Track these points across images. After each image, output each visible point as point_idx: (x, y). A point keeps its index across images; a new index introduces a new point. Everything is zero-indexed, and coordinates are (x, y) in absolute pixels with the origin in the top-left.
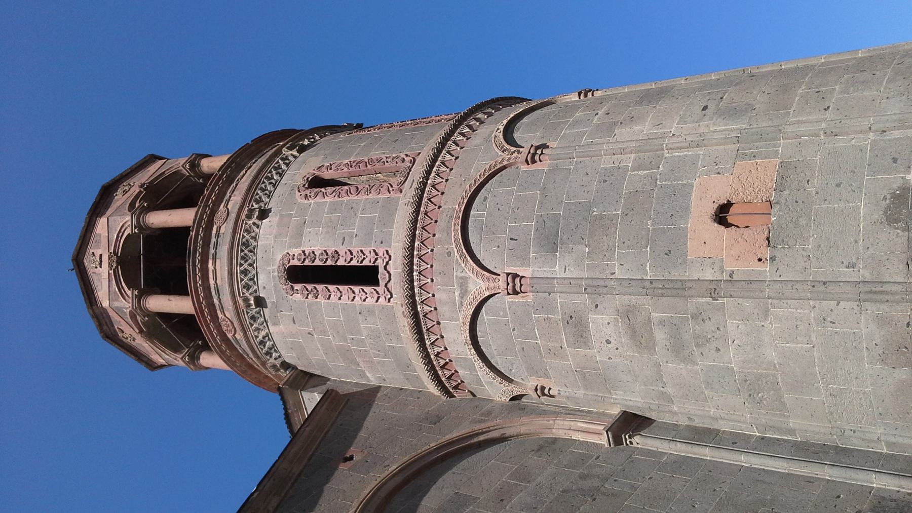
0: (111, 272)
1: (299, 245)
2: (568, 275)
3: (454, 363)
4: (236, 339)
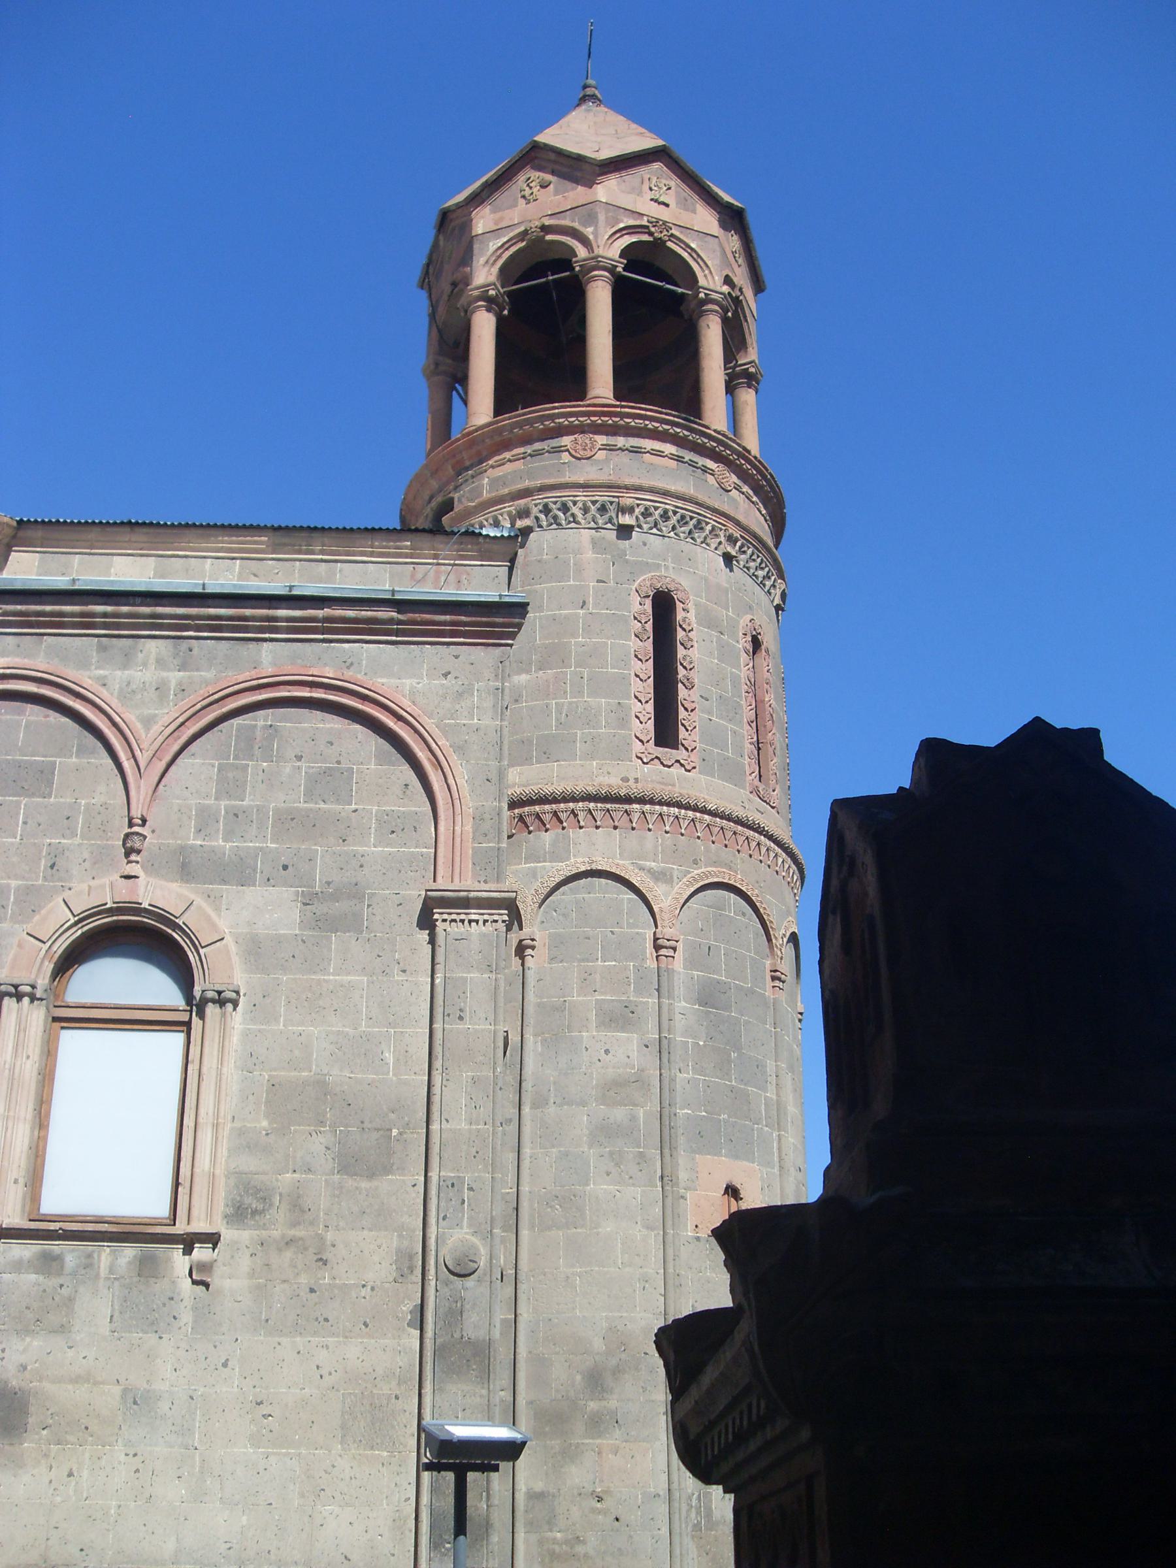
0: (644, 222)
2: (678, 1017)
3: (560, 831)
4: (562, 451)
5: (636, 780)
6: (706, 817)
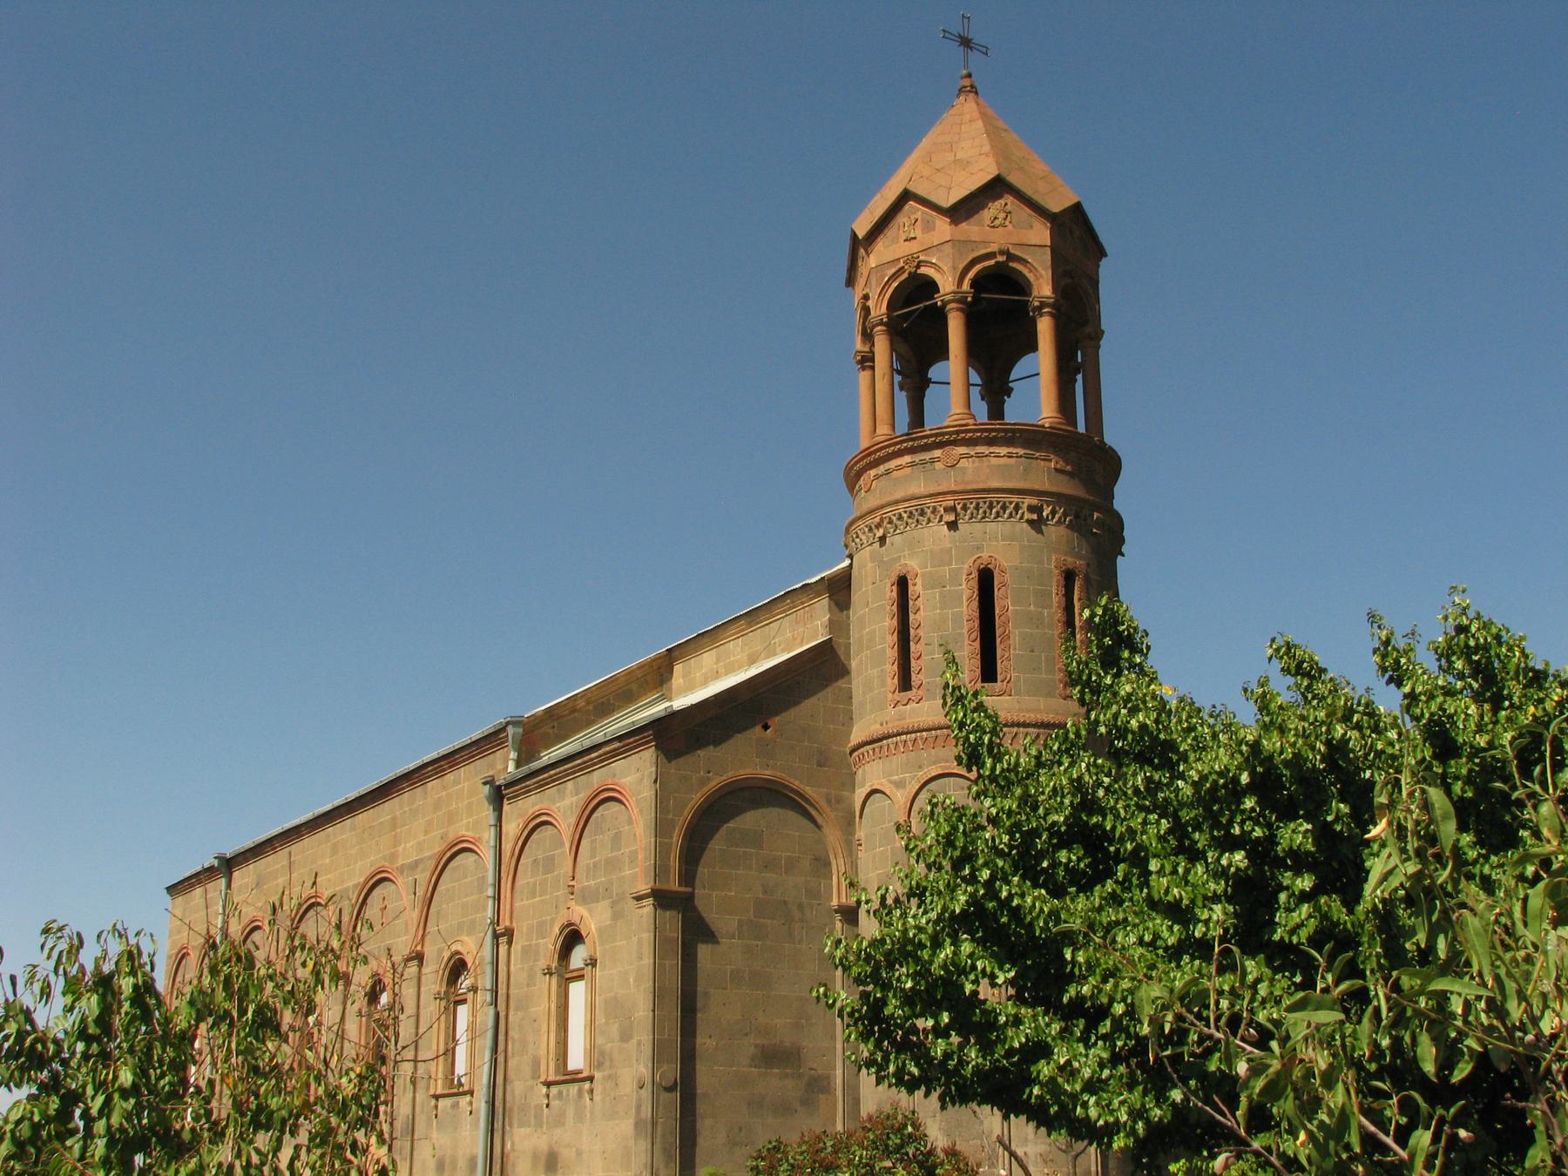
0: (902, 264)
1: (925, 588)
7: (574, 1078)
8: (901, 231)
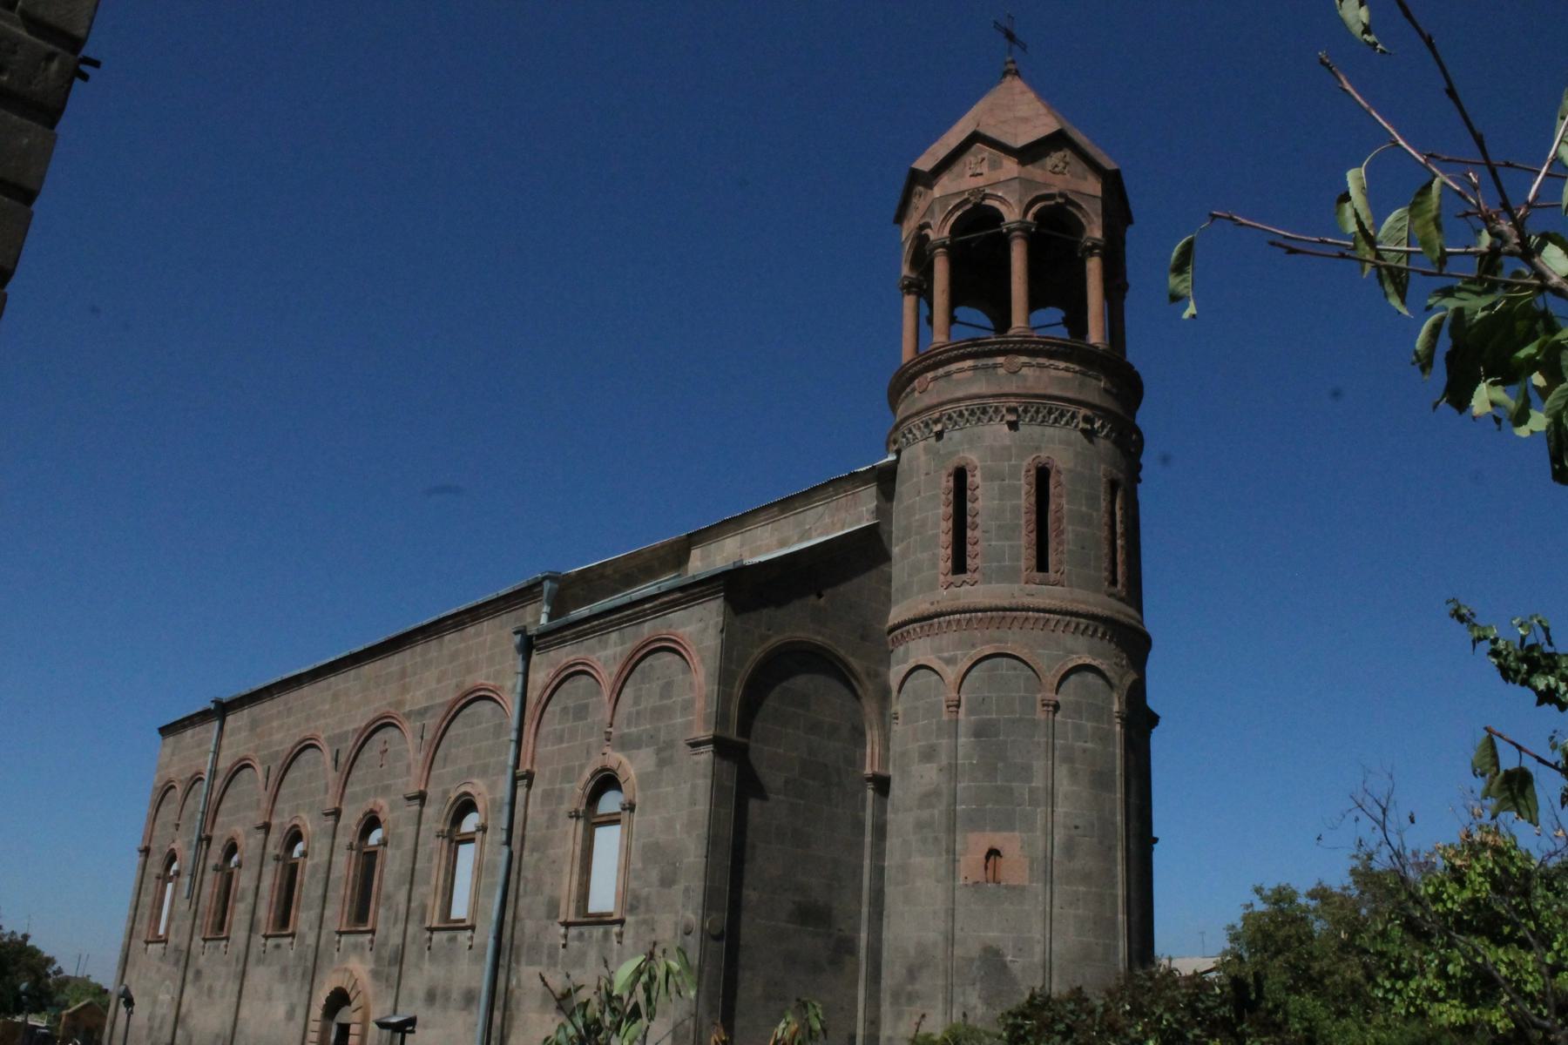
0: (966, 196)
1: (984, 479)
5: (938, 602)
6: (980, 614)
7: (601, 920)
8: (967, 168)
